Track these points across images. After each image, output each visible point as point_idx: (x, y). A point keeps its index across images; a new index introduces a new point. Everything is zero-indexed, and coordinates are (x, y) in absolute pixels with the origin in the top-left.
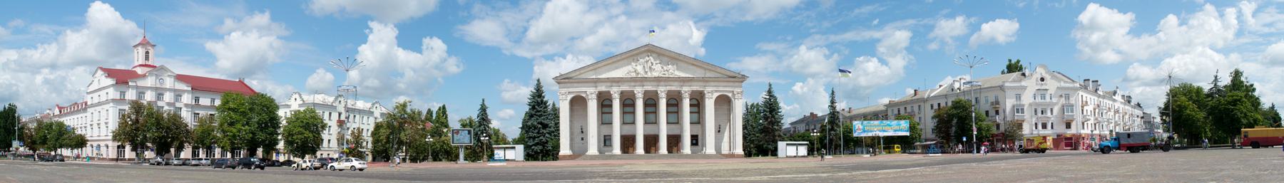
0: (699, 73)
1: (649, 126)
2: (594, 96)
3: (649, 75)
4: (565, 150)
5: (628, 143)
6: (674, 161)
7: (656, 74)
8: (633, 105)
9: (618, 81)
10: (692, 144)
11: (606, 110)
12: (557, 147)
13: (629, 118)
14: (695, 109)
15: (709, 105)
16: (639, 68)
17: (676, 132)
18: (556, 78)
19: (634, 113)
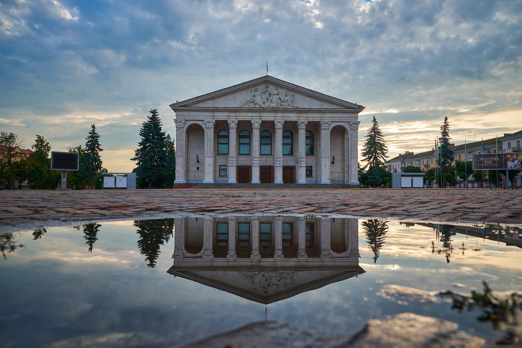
0: (316, 105)
1: (264, 158)
2: (212, 125)
3: (267, 105)
4: (179, 179)
5: (244, 174)
7: (274, 105)
8: (249, 137)
10: (307, 175)
11: (221, 140)
12: (173, 177)
13: (244, 149)
14: (309, 141)
15: (325, 136)
16: (259, 100)
17: (291, 163)
18: (172, 106)
19: (250, 144)
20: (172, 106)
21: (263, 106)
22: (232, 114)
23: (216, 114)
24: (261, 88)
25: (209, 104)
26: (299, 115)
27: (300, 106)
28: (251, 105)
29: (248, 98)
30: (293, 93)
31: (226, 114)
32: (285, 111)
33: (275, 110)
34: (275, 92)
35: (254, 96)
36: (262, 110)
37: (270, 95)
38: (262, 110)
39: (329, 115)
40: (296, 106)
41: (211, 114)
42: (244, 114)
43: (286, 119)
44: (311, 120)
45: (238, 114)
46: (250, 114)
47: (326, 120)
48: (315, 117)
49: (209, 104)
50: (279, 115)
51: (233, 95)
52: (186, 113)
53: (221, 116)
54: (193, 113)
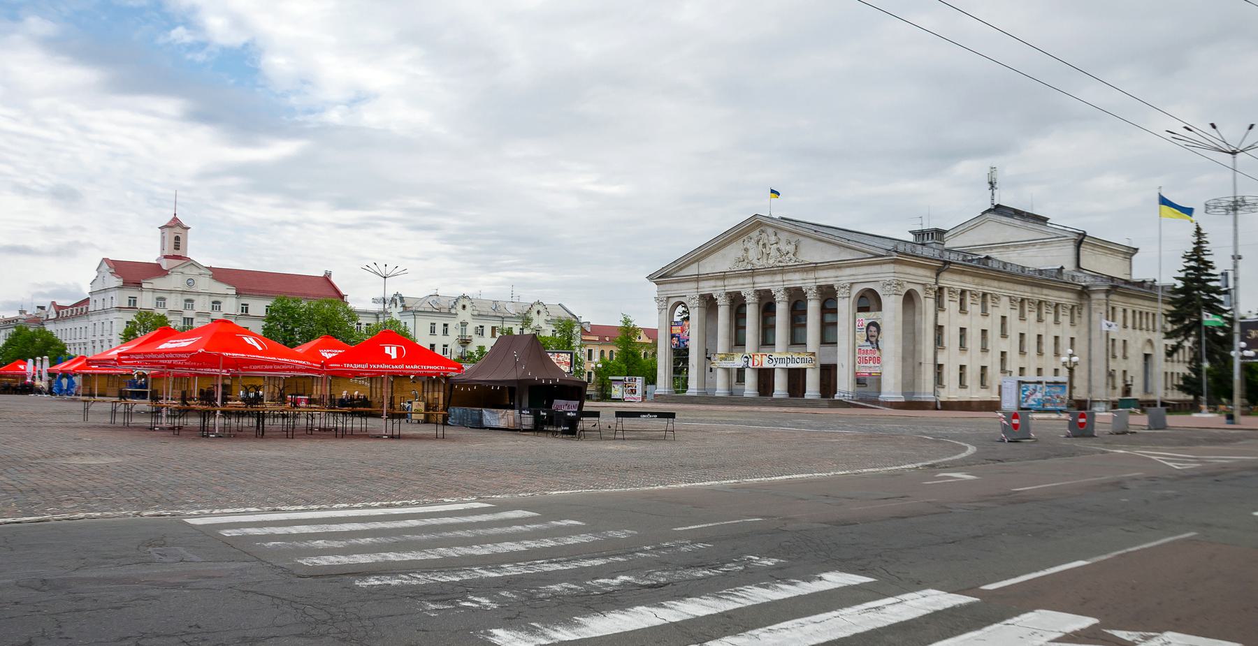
2: (695, 303)
6: (764, 405)
9: (723, 276)
18: (650, 277)
20: (650, 277)
21: (758, 265)
22: (720, 283)
23: (702, 284)
24: (754, 234)
25: (692, 270)
26: (805, 276)
27: (808, 260)
28: (742, 266)
29: (741, 254)
30: (795, 238)
31: (712, 283)
32: (783, 270)
33: (770, 272)
34: (773, 239)
35: (746, 250)
36: (753, 273)
37: (764, 245)
38: (753, 273)
39: (848, 271)
40: (801, 258)
41: (694, 285)
42: (733, 281)
43: (788, 285)
44: (822, 282)
45: (726, 282)
46: (741, 281)
47: (845, 281)
48: (826, 277)
49: (692, 270)
50: (779, 277)
51: (722, 252)
52: (668, 287)
53: (706, 287)
54: (675, 286)
